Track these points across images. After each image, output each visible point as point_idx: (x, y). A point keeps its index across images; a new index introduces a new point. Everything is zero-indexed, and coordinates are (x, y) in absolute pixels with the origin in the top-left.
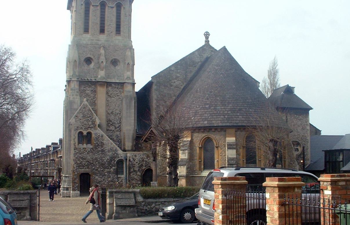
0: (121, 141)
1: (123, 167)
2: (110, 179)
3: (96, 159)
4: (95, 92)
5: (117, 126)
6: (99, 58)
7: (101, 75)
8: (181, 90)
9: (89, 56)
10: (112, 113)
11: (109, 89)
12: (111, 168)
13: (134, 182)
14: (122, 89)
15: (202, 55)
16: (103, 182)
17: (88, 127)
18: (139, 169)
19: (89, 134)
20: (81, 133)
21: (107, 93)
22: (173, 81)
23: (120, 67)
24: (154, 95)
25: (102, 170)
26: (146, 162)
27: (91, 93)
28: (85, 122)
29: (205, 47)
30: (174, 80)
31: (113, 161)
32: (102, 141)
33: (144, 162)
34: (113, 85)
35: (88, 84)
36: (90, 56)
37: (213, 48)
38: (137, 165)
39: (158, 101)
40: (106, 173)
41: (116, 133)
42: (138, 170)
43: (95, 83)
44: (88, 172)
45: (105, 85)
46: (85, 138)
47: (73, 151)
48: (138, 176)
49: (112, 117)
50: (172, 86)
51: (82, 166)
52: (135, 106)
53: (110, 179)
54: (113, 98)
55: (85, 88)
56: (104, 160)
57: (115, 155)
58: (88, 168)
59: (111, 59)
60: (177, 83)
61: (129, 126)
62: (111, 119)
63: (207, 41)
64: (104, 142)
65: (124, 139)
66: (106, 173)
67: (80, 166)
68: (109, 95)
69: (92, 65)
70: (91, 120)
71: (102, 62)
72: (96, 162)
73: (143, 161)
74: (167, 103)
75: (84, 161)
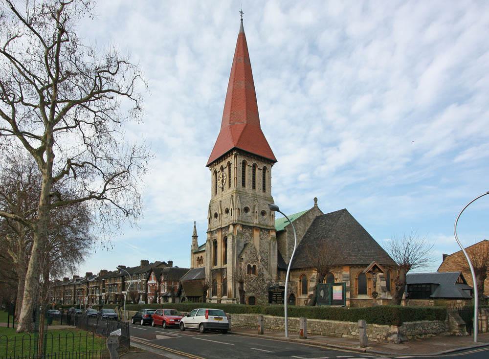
4: (252, 234)
6: (254, 209)
7: (256, 222)
9: (247, 206)
10: (263, 252)
19: (254, 266)
20: (249, 266)
22: (298, 231)
28: (252, 258)
34: (263, 231)
59: (261, 210)
61: (274, 263)
69: (249, 213)
71: (256, 212)
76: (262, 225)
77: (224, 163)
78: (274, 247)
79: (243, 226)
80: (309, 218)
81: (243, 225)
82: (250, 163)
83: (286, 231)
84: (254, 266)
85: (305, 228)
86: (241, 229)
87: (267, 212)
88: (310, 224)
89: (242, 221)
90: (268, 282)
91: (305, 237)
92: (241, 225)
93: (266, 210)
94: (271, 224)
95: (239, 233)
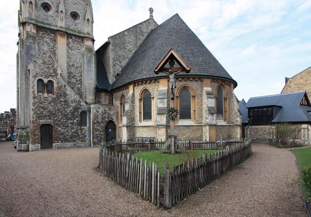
0: (82, 94)
1: (86, 118)
2: (73, 131)
3: (59, 110)
4: (55, 41)
5: (78, 79)
8: (133, 54)
10: (73, 65)
11: (70, 42)
12: (75, 119)
13: (98, 133)
14: (82, 43)
15: (148, 27)
16: (66, 133)
17: (48, 74)
18: (102, 121)
19: (51, 82)
20: (40, 81)
21: (68, 45)
24: (111, 54)
25: (65, 121)
26: (108, 114)
27: (51, 42)
28: (46, 70)
29: (150, 21)
30: (127, 44)
31: (76, 113)
32: (64, 91)
33: (107, 114)
34: (73, 38)
35: (47, 32)
36: (48, 2)
38: (101, 117)
39: (114, 60)
40: (69, 125)
41: (77, 86)
42: (101, 121)
44: (50, 123)
45: (65, 36)
46: (45, 86)
47: (31, 101)
48: (101, 127)
49: (73, 70)
50: (125, 49)
51: (42, 117)
52: (95, 62)
53: (73, 131)
54: (73, 51)
55: (43, 35)
56: (67, 111)
57: (79, 106)
58: (50, 119)
59: (70, 11)
60: (130, 47)
61: (90, 80)
62: (72, 72)
64: (67, 92)
65: (86, 91)
66: (69, 125)
67: (39, 117)
68: (70, 47)
70: (53, 68)
71: (62, 11)
72: (58, 113)
73: (106, 113)
74: (122, 63)
75: (46, 111)
76: (72, 31)
78: (89, 62)
79: (38, 28)
80: (141, 31)
81: (37, 26)
84: (51, 82)
85: (136, 42)
86: (34, 31)
87: (80, 14)
88: (143, 38)
89: (36, 20)
90: (74, 105)
91: (135, 53)
92: (34, 25)
93: (78, 12)
94: (86, 30)
95: (29, 35)
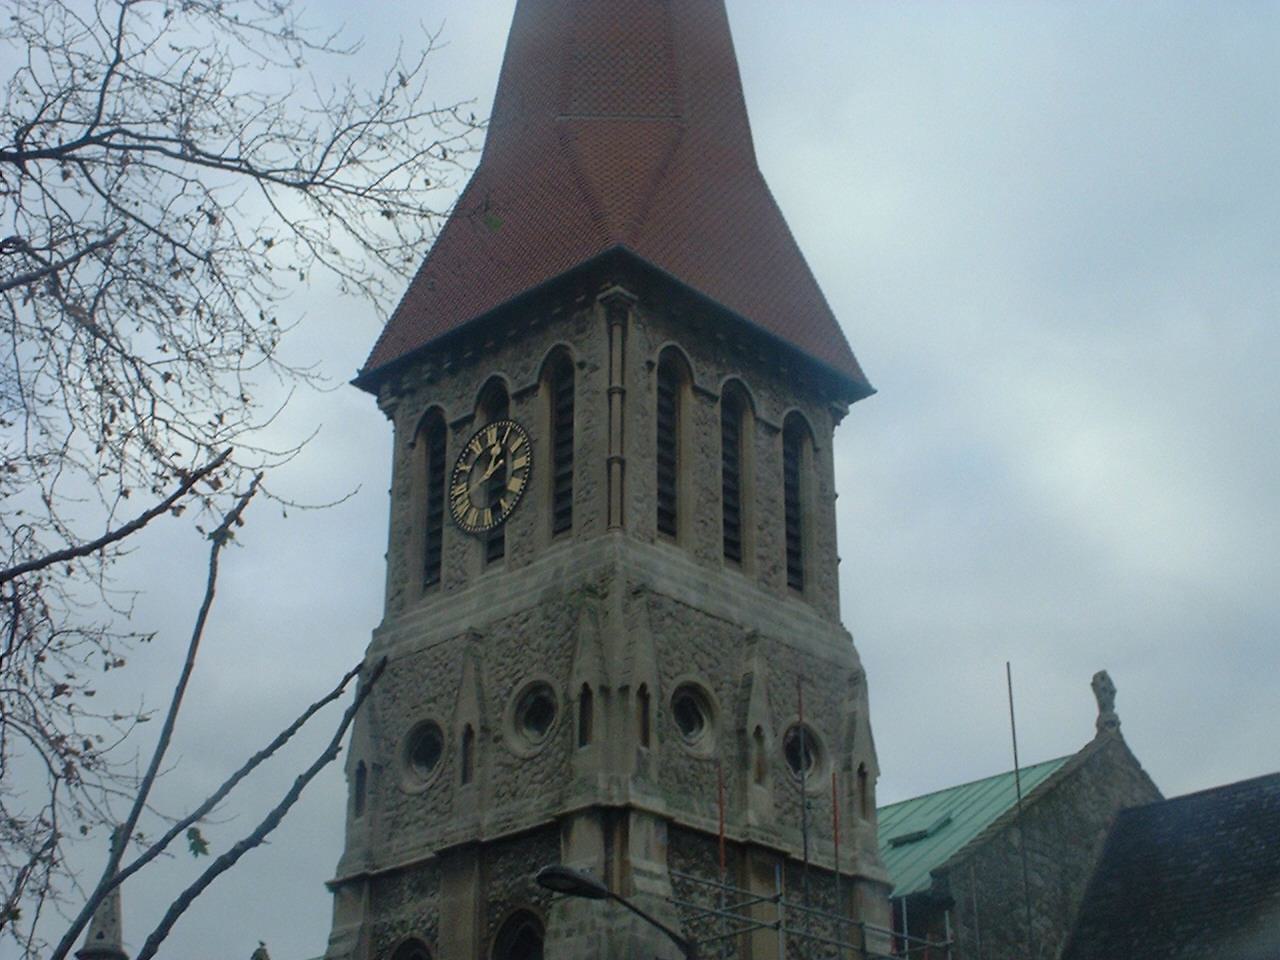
6: (742, 707)
9: (693, 677)
23: (819, 781)
37: (1136, 764)
43: (745, 856)
63: (1108, 723)
69: (705, 742)
71: (759, 729)
77: (517, 370)
82: (710, 376)
83: (948, 903)
